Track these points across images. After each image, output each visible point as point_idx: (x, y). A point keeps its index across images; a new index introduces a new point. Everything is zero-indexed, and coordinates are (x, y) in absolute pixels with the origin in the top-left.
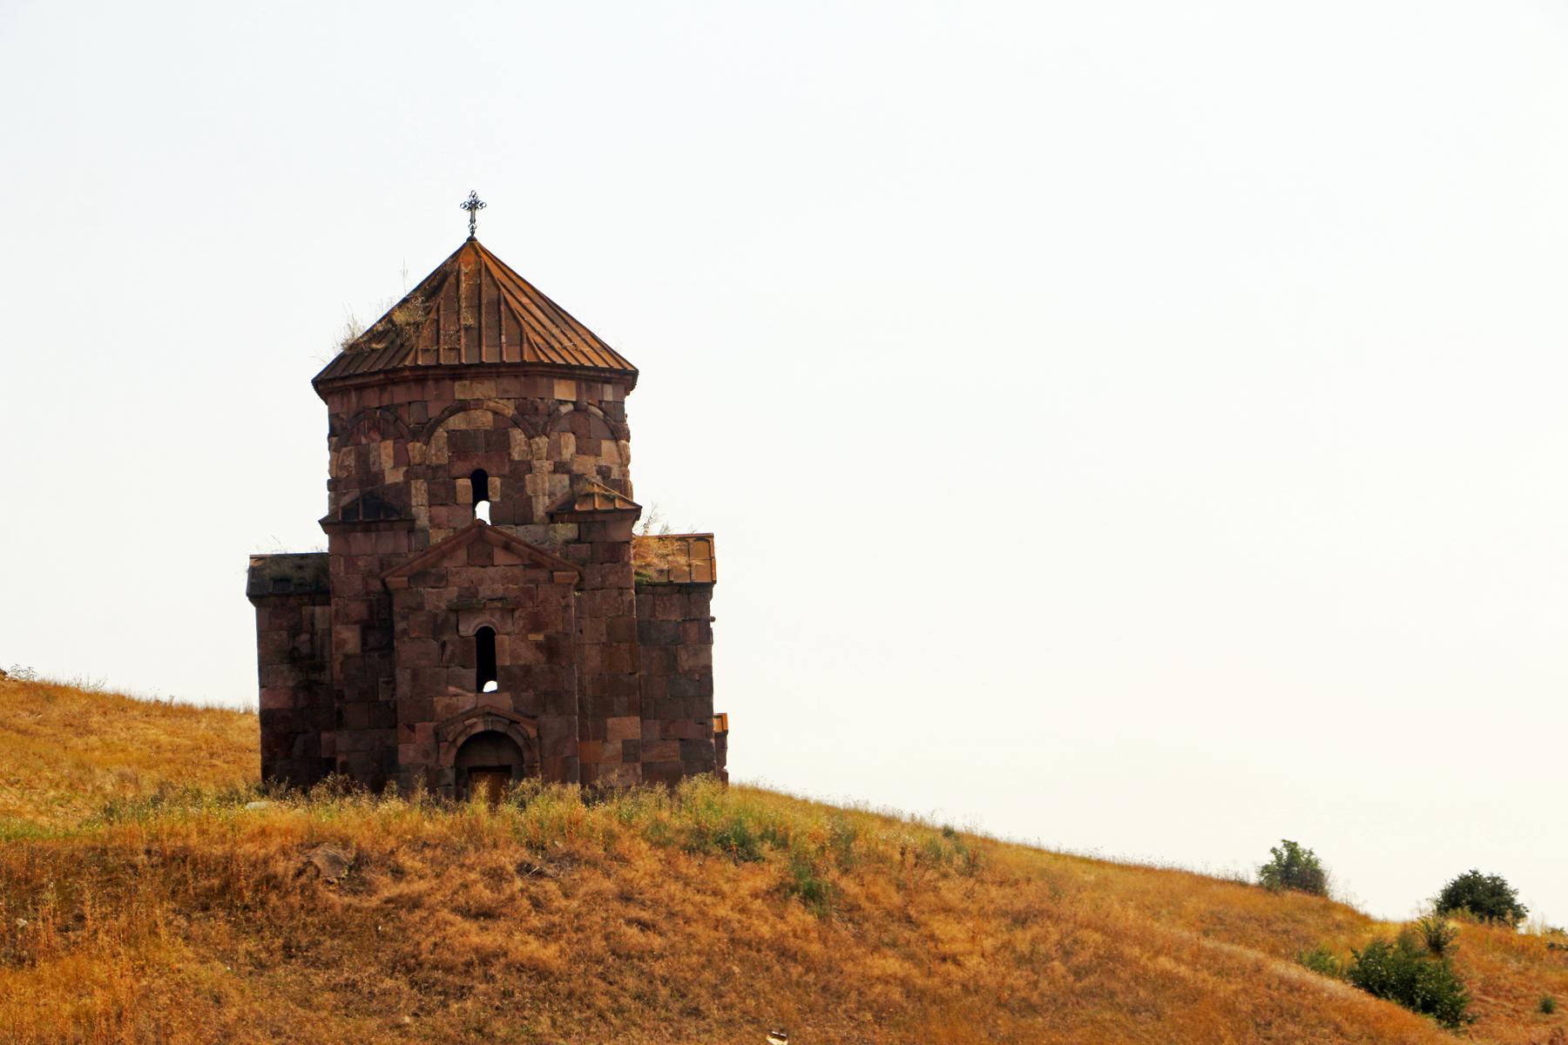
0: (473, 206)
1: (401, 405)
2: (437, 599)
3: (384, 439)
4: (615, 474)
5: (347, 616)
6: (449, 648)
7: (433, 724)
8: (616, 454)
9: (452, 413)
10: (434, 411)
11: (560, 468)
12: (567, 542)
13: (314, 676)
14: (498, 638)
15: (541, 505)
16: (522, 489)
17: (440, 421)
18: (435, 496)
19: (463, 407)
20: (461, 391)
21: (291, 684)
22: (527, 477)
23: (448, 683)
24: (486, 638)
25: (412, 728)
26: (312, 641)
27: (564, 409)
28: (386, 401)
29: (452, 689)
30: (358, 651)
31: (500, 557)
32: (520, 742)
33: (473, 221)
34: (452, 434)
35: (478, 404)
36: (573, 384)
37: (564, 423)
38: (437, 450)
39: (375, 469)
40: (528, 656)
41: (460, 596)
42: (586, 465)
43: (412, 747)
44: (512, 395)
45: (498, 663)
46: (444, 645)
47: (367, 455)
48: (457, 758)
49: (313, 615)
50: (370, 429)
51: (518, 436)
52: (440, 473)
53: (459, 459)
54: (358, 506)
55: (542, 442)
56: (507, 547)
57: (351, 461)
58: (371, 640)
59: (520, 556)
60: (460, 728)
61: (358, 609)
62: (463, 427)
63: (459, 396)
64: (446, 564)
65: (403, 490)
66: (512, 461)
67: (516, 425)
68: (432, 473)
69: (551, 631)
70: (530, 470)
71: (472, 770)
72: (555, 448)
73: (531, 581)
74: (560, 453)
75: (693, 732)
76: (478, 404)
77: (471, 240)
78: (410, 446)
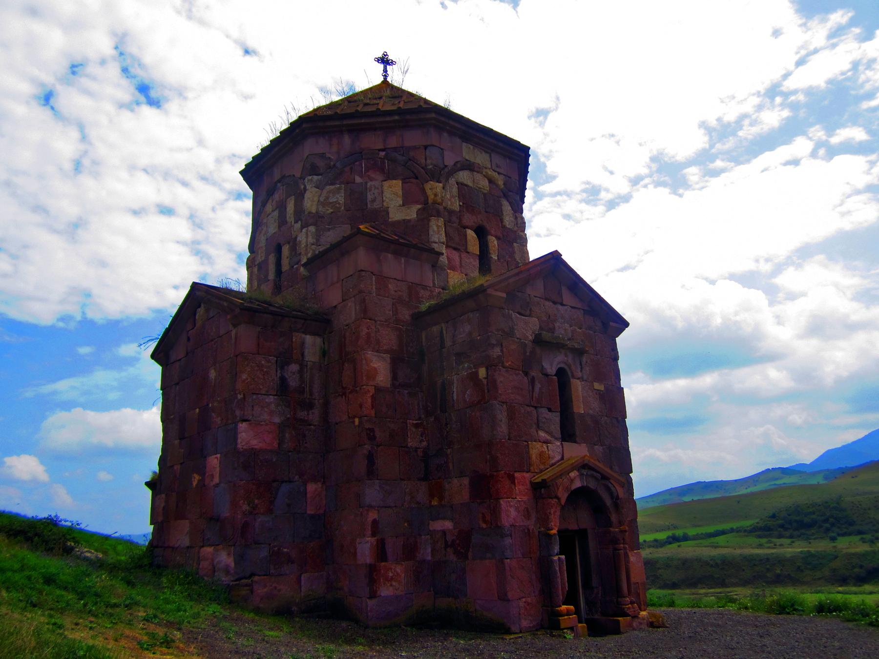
1: (415, 148)
3: (389, 177)
6: (538, 386)
9: (462, 169)
10: (450, 160)
13: (302, 414)
16: (512, 254)
19: (469, 167)
20: (469, 153)
21: (277, 420)
22: (515, 244)
23: (539, 427)
25: (512, 478)
26: (301, 372)
28: (393, 142)
29: (542, 434)
32: (608, 502)
33: (385, 71)
34: (461, 185)
39: (376, 205)
43: (513, 502)
44: (501, 171)
45: (575, 410)
46: (532, 381)
49: (303, 344)
50: (367, 170)
57: (340, 198)
61: (389, 338)
66: (504, 227)
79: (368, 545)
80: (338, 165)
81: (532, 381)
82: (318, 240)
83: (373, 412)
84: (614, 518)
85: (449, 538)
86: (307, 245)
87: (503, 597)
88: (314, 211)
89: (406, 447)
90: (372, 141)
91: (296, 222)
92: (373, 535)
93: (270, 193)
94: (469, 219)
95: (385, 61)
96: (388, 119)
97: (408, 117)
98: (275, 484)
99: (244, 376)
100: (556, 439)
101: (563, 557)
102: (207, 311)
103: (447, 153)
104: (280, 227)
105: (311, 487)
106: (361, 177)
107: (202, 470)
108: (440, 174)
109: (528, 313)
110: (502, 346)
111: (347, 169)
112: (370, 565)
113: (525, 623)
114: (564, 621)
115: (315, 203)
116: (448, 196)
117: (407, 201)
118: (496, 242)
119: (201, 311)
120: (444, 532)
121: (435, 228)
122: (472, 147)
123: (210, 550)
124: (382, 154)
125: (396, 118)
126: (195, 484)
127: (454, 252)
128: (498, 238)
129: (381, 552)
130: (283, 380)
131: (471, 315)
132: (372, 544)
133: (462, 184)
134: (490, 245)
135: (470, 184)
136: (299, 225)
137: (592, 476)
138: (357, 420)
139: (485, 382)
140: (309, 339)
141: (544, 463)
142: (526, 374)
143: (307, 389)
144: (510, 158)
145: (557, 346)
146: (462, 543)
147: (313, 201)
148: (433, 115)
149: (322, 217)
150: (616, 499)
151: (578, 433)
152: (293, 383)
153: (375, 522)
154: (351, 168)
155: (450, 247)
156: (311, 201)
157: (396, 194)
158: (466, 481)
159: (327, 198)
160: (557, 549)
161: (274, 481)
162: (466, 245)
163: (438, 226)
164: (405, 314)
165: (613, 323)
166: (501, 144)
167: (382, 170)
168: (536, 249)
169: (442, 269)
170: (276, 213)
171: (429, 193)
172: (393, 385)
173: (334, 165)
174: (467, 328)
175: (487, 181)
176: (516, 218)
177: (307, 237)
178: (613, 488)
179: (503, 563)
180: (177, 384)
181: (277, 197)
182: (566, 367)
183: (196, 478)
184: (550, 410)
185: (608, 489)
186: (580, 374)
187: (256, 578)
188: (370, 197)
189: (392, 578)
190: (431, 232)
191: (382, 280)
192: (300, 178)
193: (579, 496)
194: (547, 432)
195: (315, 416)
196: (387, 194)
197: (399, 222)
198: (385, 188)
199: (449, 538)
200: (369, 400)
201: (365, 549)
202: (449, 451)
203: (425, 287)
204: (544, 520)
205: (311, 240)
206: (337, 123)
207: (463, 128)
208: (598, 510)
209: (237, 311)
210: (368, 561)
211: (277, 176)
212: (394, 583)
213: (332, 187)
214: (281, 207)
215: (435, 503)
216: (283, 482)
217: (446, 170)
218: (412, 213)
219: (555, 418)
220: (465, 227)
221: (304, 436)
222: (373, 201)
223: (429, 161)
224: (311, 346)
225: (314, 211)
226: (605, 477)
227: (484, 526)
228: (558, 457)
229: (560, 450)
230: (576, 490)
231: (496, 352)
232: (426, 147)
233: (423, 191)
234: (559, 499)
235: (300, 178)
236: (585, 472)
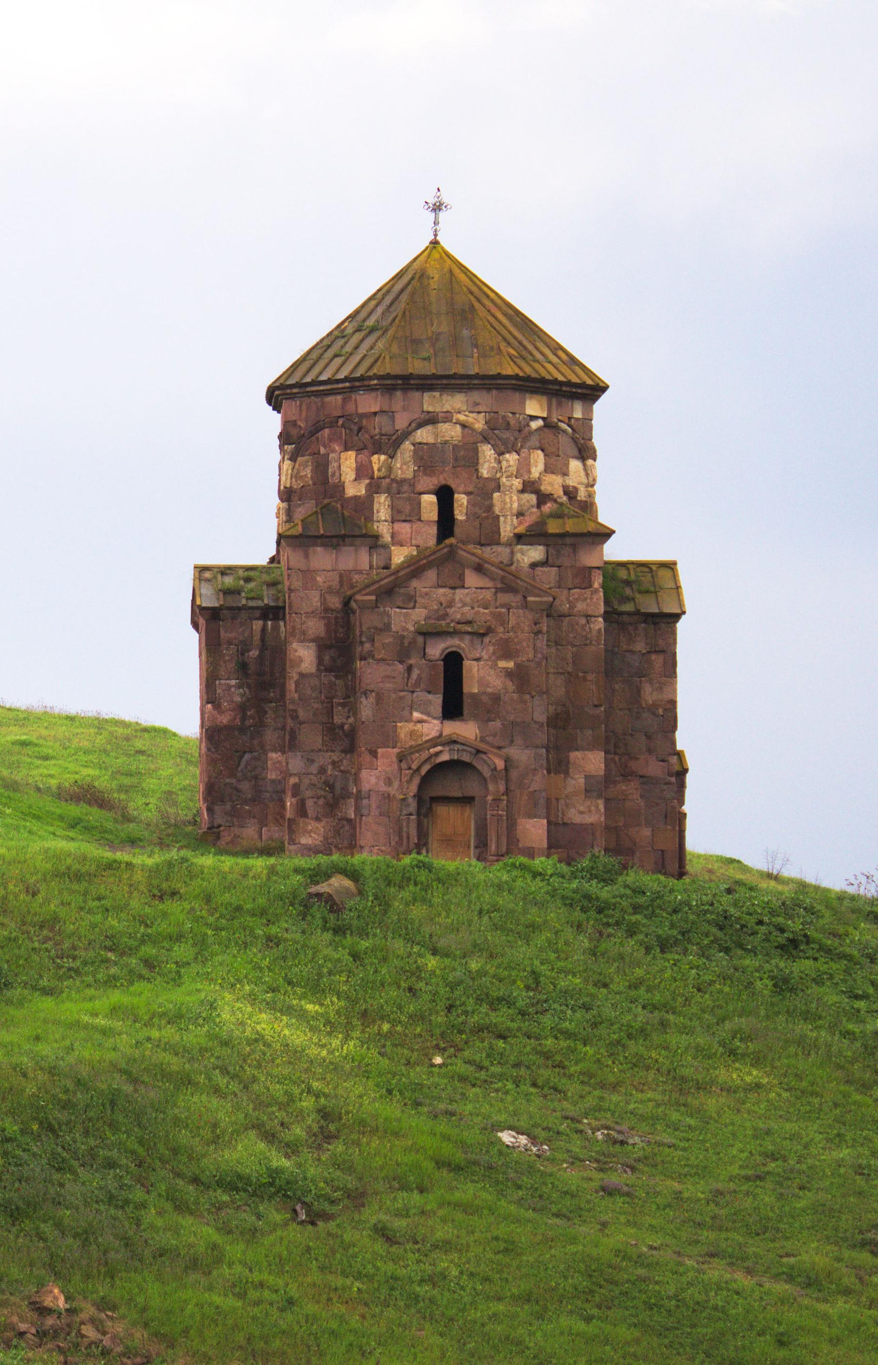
0: (437, 208)
2: (405, 620)
4: (582, 495)
5: (304, 633)
7: (396, 750)
8: (583, 473)
9: (420, 426)
10: (401, 423)
11: (529, 487)
12: (534, 565)
14: (466, 663)
15: (508, 528)
16: (490, 508)
17: (406, 434)
18: (399, 512)
20: (431, 402)
22: (496, 495)
23: (412, 708)
24: (453, 664)
25: (374, 754)
27: (534, 425)
29: (416, 715)
30: (313, 670)
31: (472, 579)
32: (487, 773)
33: (436, 223)
35: (447, 417)
36: (544, 399)
37: (534, 441)
38: (404, 464)
40: (497, 683)
41: (427, 618)
42: (553, 484)
44: (480, 408)
45: (466, 690)
46: (409, 669)
47: (326, 465)
48: (421, 786)
50: (330, 440)
51: (487, 452)
52: (405, 488)
53: (425, 474)
54: (316, 516)
55: (511, 458)
56: (479, 569)
57: (308, 472)
59: (493, 579)
60: (425, 755)
61: (315, 627)
62: (431, 440)
64: (415, 583)
65: (364, 506)
67: (486, 439)
69: (522, 658)
70: (498, 488)
71: (434, 799)
72: (524, 466)
73: (502, 606)
74: (529, 472)
75: (654, 768)
76: (447, 417)
77: (435, 243)
92: (294, 796)
106: (325, 447)
116: (398, 465)
122: (437, 394)
127: (404, 524)
128: (468, 494)
134: (455, 505)
141: (415, 740)
148: (375, 382)
164: (335, 602)
169: (385, 547)
172: (318, 670)
176: (500, 462)
184: (429, 692)
194: (422, 713)
203: (360, 572)
219: (437, 700)
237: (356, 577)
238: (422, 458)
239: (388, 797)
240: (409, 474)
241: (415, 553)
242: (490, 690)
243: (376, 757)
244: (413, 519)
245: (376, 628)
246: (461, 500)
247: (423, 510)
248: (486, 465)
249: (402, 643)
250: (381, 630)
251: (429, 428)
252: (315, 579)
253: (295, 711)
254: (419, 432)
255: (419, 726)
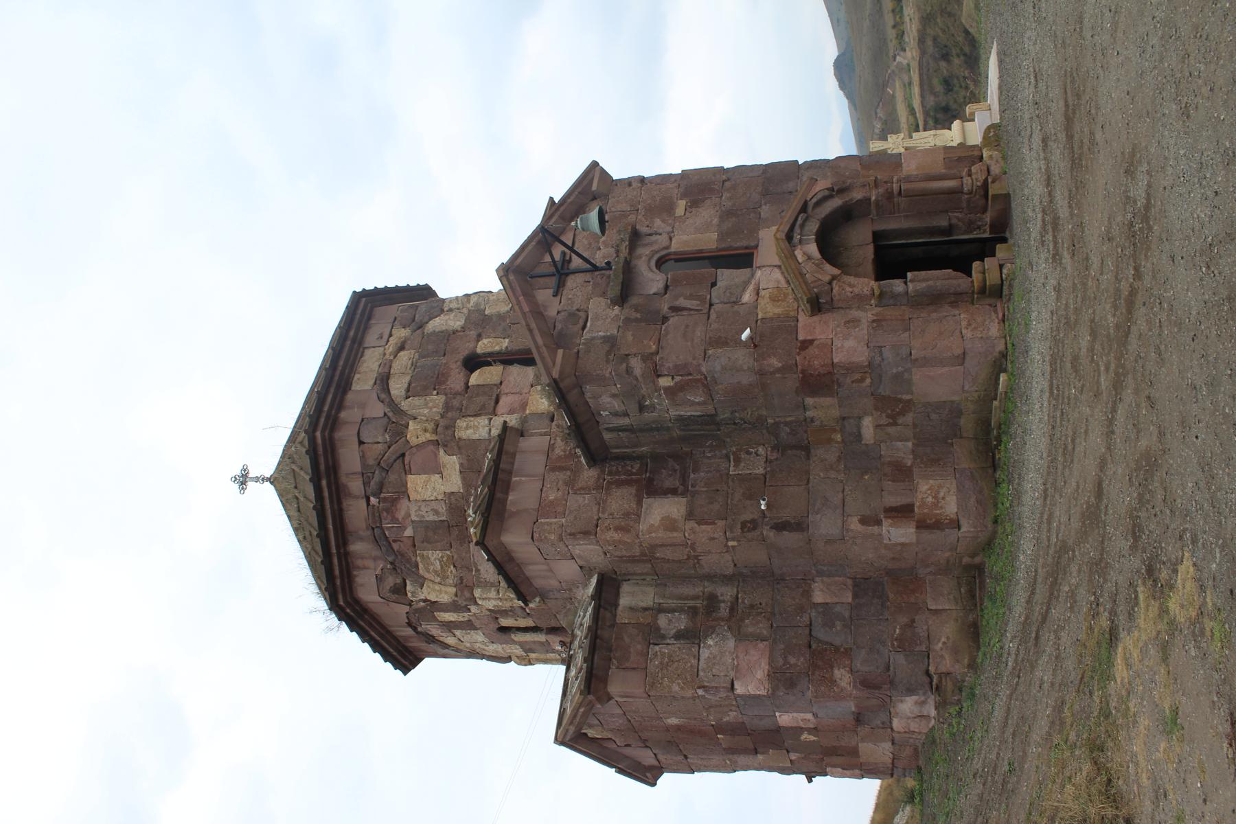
1: (363, 457)
3: (403, 492)
5: (627, 515)
6: (682, 302)
7: (803, 318)
10: (377, 410)
13: (724, 611)
19: (384, 381)
20: (364, 382)
21: (731, 643)
25: (805, 345)
29: (747, 297)
30: (684, 500)
32: (836, 202)
33: (257, 479)
39: (442, 509)
46: (675, 309)
49: (631, 609)
52: (456, 403)
57: (435, 556)
58: (668, 483)
61: (620, 500)
63: (368, 385)
68: (452, 412)
78: (414, 441)
79: (892, 530)
80: (390, 559)
81: (675, 309)
82: (492, 585)
83: (721, 523)
84: (857, 195)
85: (884, 421)
86: (500, 599)
87: (962, 358)
88: (454, 590)
89: (765, 476)
90: (357, 512)
91: (469, 610)
92: (879, 523)
93: (431, 639)
94: (456, 380)
95: (243, 480)
96: (326, 494)
97: (322, 467)
98: (814, 646)
99: (676, 688)
100: (753, 276)
101: (909, 275)
102: (591, 726)
103: (369, 414)
104: (476, 629)
105: (818, 597)
107: (798, 730)
108: (396, 423)
109: (582, 314)
110: (627, 355)
111: (395, 546)
112: (917, 527)
113: (994, 330)
114: (993, 278)
115: (443, 588)
116: (426, 411)
117: (438, 470)
118: (485, 341)
119: (591, 733)
120: (877, 426)
121: (470, 432)
122: (357, 376)
123: (896, 724)
124: (373, 500)
125: (324, 483)
126: (812, 738)
127: (501, 403)
128: (479, 337)
129: (903, 512)
130: (679, 636)
131: (588, 395)
132: (891, 525)
133: (408, 390)
134: (489, 350)
135: (408, 379)
136: (473, 609)
137: (802, 226)
138: (730, 543)
139: (678, 379)
140: (624, 601)
141: (786, 295)
142: (665, 319)
143: (691, 603)
144: (369, 318)
145: (628, 270)
146: (892, 407)
147: (440, 591)
148: (318, 434)
149: (461, 578)
150: (832, 193)
151: (744, 243)
152: (682, 622)
153: (864, 521)
154: (394, 541)
155: (495, 408)
156: (443, 594)
157: (426, 484)
158: (810, 401)
159: (436, 572)
160: (897, 285)
161: (810, 647)
162: (490, 386)
163: (467, 428)
164: (589, 474)
165: (593, 187)
166: (352, 333)
167: (394, 502)
168: (496, 286)
170: (458, 633)
171: (422, 439)
172: (683, 494)
173: (391, 563)
174: (606, 399)
175: (402, 353)
176: (451, 310)
177: (489, 599)
178: (819, 196)
179: (916, 360)
180: (686, 757)
181: (435, 631)
182: (656, 258)
183: (805, 737)
184: (714, 284)
185: (818, 204)
186: (665, 238)
187: (932, 669)
188: (431, 517)
189: (935, 497)
190: (476, 437)
191: (545, 509)
192: (410, 605)
193: (829, 248)
194: (744, 290)
195: (726, 593)
196: (428, 494)
197: (464, 479)
198: (419, 498)
199: (884, 421)
200: (704, 527)
201: (900, 534)
202: (770, 421)
203: (551, 447)
204: (860, 300)
205: (493, 594)
206: (335, 561)
207: (332, 390)
208: (847, 215)
209: (591, 697)
210: (913, 530)
211: (410, 631)
212: (942, 494)
213: (421, 566)
214: (450, 627)
215: (838, 437)
216: (810, 635)
217: (390, 414)
218: (452, 463)
219: (726, 277)
220: (467, 387)
221: (752, 606)
222: (436, 512)
223: (380, 439)
224: (631, 597)
225: (454, 590)
226: (804, 209)
227: (868, 381)
228: (777, 274)
229: (768, 270)
230: (822, 250)
231: (637, 365)
232: (361, 443)
233: (419, 446)
234: (834, 278)
235: (410, 605)
236: (797, 237)
237: (558, 451)
238: (425, 388)
239: (878, 322)
240: (441, 399)
241: (539, 388)
242: (716, 221)
243: (811, 342)
244: (496, 391)
245: (608, 353)
246: (485, 346)
247: (489, 381)
248: (451, 323)
249: (636, 320)
250: (613, 346)
251: (392, 383)
252: (552, 502)
253: (744, 525)
254: (392, 392)
255: (762, 293)
